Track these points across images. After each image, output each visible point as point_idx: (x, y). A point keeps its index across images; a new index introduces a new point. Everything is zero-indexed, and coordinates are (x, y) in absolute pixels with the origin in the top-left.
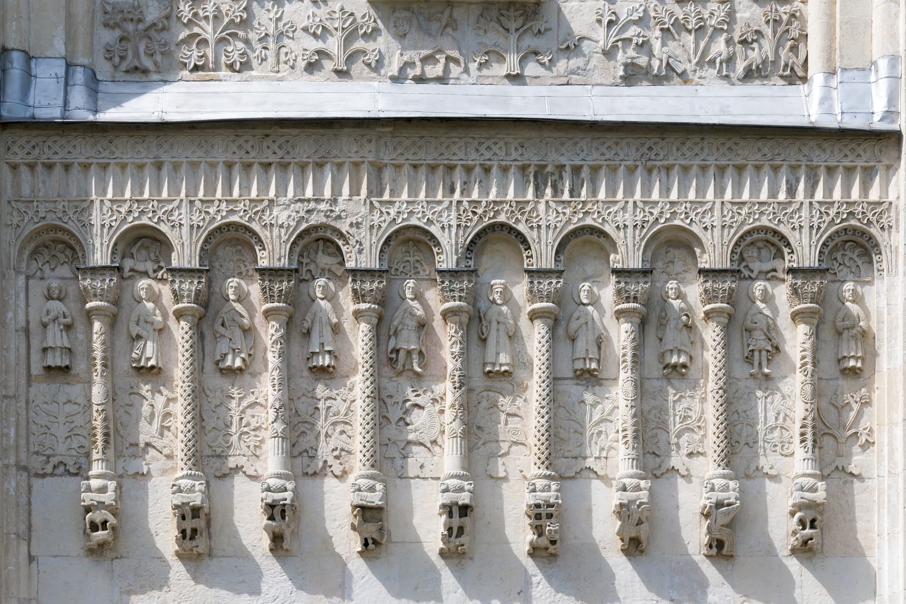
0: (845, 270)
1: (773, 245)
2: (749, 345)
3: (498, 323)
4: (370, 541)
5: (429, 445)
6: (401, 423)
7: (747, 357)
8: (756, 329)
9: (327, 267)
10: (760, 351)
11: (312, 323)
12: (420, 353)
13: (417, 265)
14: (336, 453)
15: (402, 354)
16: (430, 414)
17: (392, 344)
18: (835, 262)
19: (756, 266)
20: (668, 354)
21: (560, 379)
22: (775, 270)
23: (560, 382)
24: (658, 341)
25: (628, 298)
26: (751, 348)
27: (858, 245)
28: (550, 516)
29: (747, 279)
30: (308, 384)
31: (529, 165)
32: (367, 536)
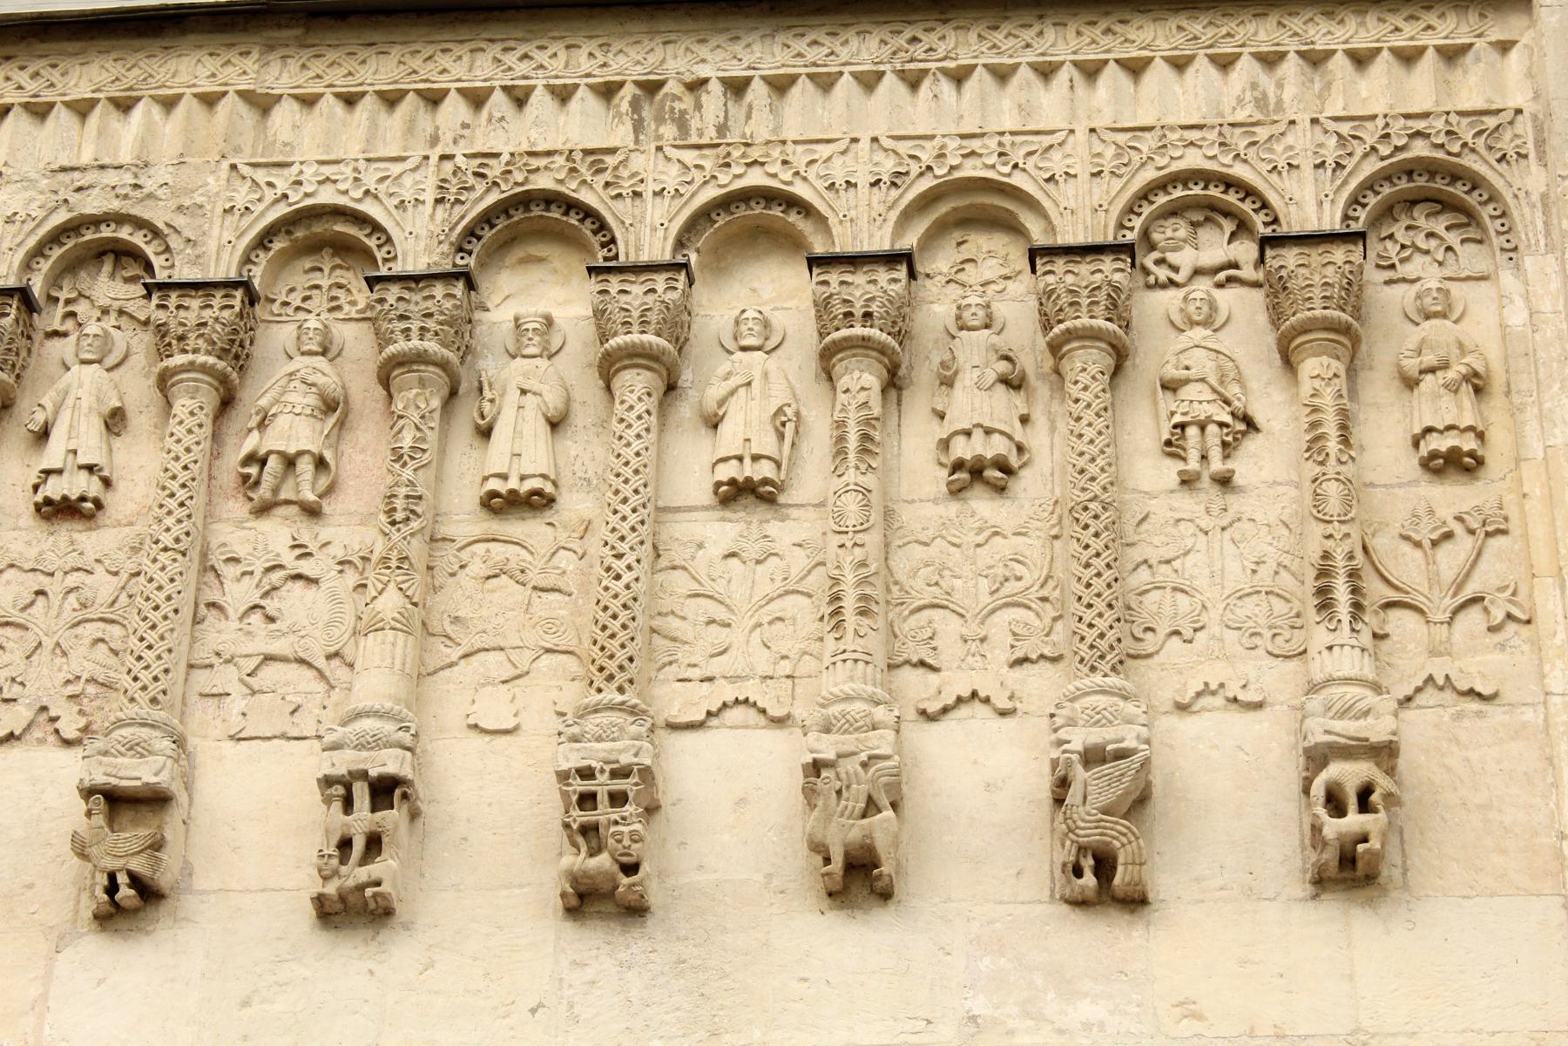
0: (1419, 259)
1: (1228, 214)
2: (1173, 414)
3: (524, 392)
4: (122, 879)
5: (320, 662)
6: (256, 618)
7: (1168, 443)
8: (1187, 381)
9: (116, 304)
10: (1203, 428)
11: (56, 412)
12: (321, 463)
13: (340, 293)
14: (71, 689)
15: (273, 462)
16: (334, 598)
17: (251, 443)
18: (1389, 244)
19: (1185, 259)
20: (961, 439)
21: (678, 510)
22: (1236, 266)
23: (678, 516)
24: (937, 420)
25: (848, 315)
26: (1177, 419)
27: (1445, 205)
28: (618, 799)
29: (1163, 287)
30: (29, 543)
31: (621, 85)
32: (110, 863)
